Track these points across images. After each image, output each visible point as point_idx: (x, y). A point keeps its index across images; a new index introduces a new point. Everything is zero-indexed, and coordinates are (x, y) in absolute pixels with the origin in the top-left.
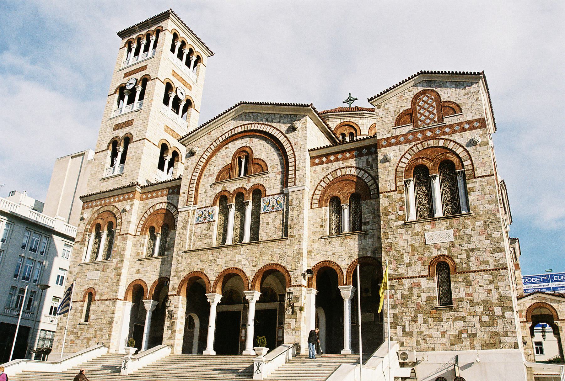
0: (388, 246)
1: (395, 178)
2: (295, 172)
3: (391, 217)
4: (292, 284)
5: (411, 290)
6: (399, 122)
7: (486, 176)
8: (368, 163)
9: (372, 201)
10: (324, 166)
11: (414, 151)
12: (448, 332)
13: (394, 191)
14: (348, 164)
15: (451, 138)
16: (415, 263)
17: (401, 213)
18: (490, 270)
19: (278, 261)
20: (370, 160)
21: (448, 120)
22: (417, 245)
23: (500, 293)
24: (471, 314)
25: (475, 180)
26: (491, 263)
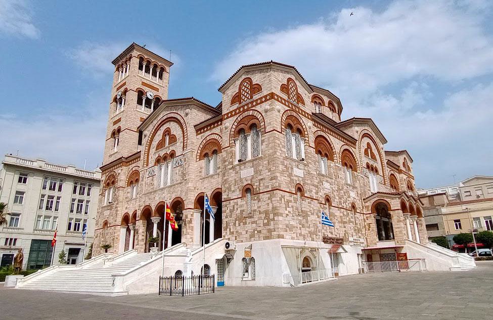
5: (234, 206)
6: (233, 102)
10: (202, 134)
12: (249, 231)
14: (212, 132)
15: (256, 109)
17: (231, 160)
21: (256, 97)
24: (260, 218)
25: (265, 135)
26: (270, 187)
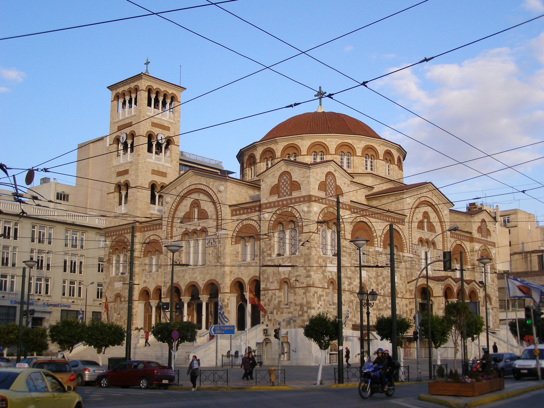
0: (263, 271)
5: (272, 297)
17: (269, 252)
21: (295, 194)
23: (307, 300)
24: (295, 310)
25: (303, 234)
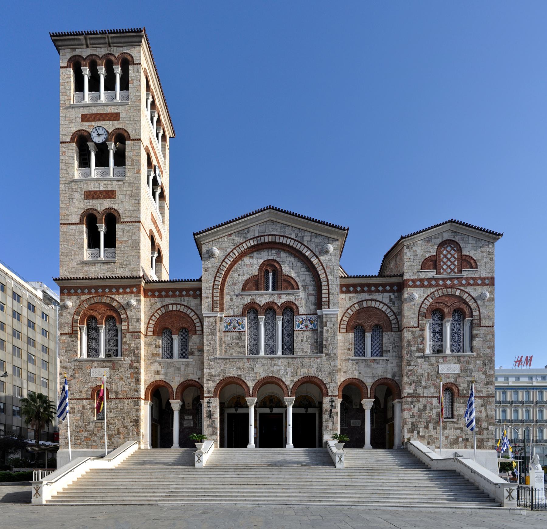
0: (410, 371)
1: (418, 317)
2: (329, 296)
3: (413, 349)
4: (329, 395)
5: (425, 406)
7: (488, 326)
8: (391, 300)
9: (393, 333)
11: (435, 296)
12: (450, 437)
13: (416, 327)
14: (373, 297)
15: (466, 290)
16: (430, 387)
17: (421, 346)
18: (482, 397)
19: (315, 374)
20: (393, 297)
22: (432, 373)
23: (487, 414)
25: (480, 328)
